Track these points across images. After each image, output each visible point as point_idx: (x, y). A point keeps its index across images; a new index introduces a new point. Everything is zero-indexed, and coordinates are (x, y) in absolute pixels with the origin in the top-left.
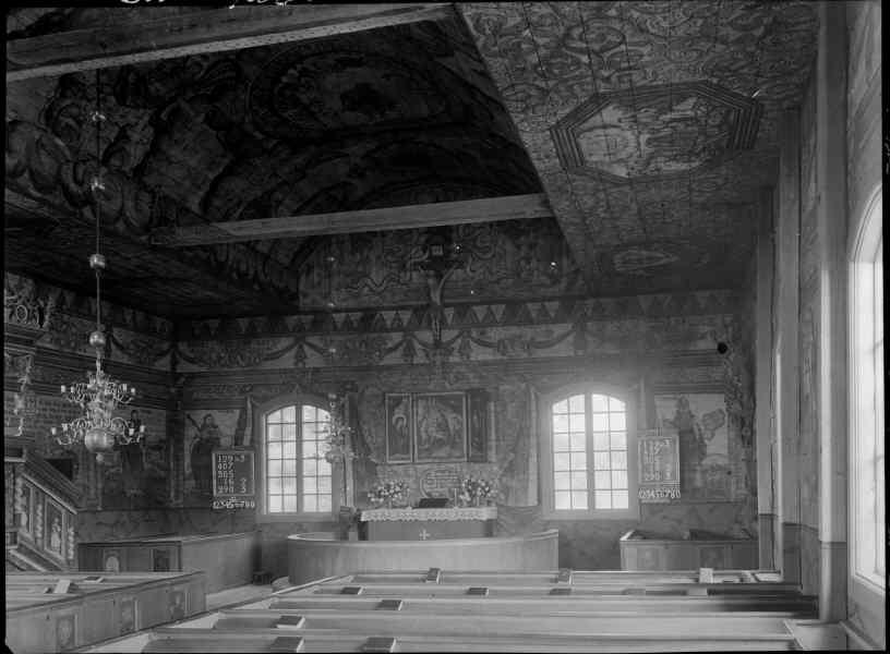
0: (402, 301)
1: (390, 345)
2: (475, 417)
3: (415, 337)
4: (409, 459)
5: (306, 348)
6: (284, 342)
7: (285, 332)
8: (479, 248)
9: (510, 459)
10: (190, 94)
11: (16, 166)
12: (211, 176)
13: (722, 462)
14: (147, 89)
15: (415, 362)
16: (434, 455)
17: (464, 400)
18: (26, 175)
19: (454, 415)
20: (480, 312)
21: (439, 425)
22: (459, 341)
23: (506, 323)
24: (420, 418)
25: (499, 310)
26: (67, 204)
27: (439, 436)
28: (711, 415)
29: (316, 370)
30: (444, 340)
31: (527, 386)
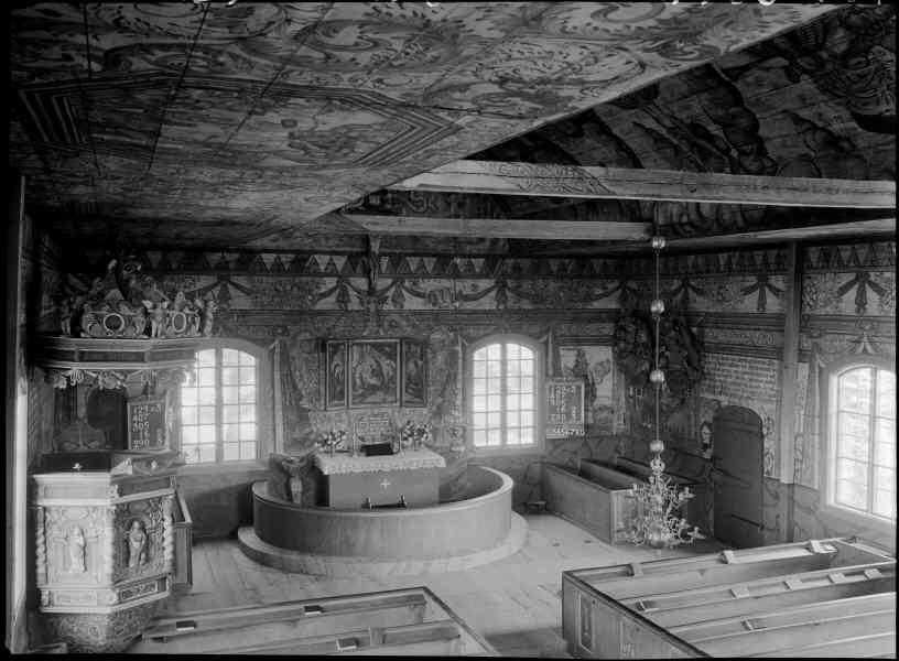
0: (337, 246)
1: (323, 290)
2: (411, 365)
3: (350, 284)
5: (229, 286)
6: (204, 281)
7: (205, 269)
8: (413, 203)
13: (608, 403)
15: (350, 309)
20: (413, 263)
22: (393, 289)
23: (438, 276)
25: (430, 263)
27: (373, 381)
28: (601, 364)
29: (243, 313)
30: (379, 288)
31: (456, 336)
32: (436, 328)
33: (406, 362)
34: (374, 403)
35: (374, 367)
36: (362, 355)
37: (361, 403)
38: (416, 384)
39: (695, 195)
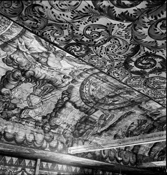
10: (143, 132)
11: (106, 157)
12: (150, 147)
14: (133, 133)
18: (108, 158)
26: (117, 163)
39: (121, 145)
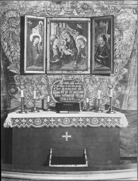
2: (101, 39)
4: (43, 70)
9: (124, 73)
16: (63, 68)
17: (89, 24)
19: (80, 37)
21: (68, 44)
24: (52, 37)
27: (67, 52)
32: (122, 10)
33: (96, 37)
34: (68, 70)
35: (68, 41)
36: (59, 32)
37: (57, 69)
38: (104, 54)
